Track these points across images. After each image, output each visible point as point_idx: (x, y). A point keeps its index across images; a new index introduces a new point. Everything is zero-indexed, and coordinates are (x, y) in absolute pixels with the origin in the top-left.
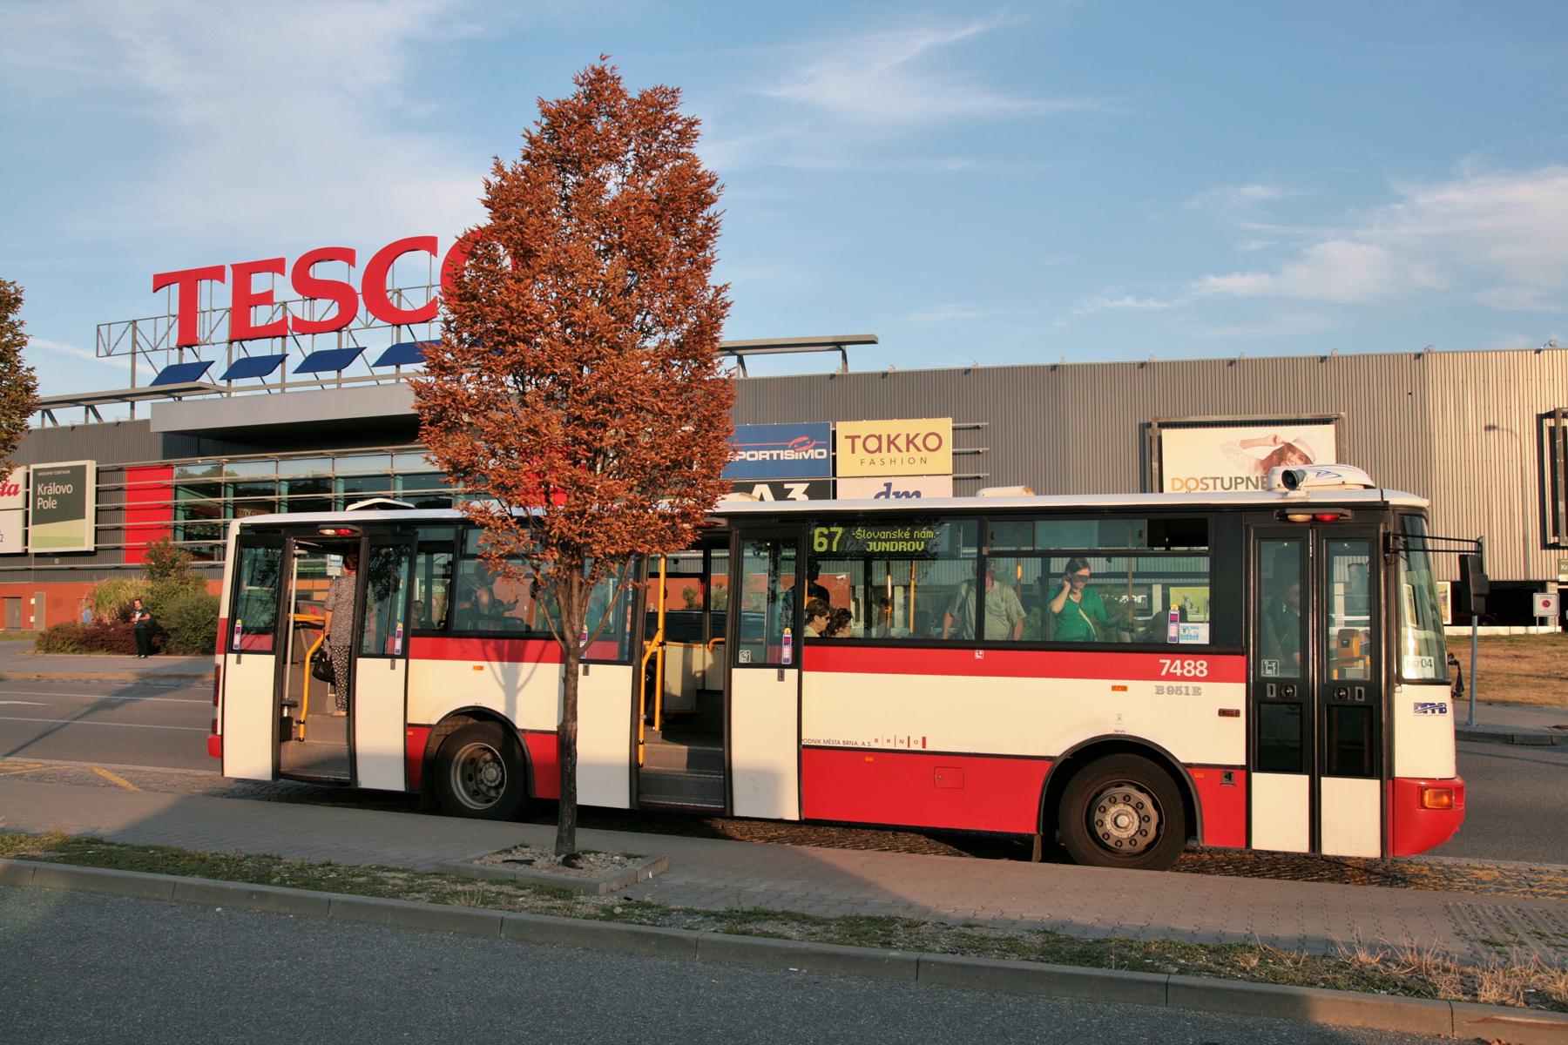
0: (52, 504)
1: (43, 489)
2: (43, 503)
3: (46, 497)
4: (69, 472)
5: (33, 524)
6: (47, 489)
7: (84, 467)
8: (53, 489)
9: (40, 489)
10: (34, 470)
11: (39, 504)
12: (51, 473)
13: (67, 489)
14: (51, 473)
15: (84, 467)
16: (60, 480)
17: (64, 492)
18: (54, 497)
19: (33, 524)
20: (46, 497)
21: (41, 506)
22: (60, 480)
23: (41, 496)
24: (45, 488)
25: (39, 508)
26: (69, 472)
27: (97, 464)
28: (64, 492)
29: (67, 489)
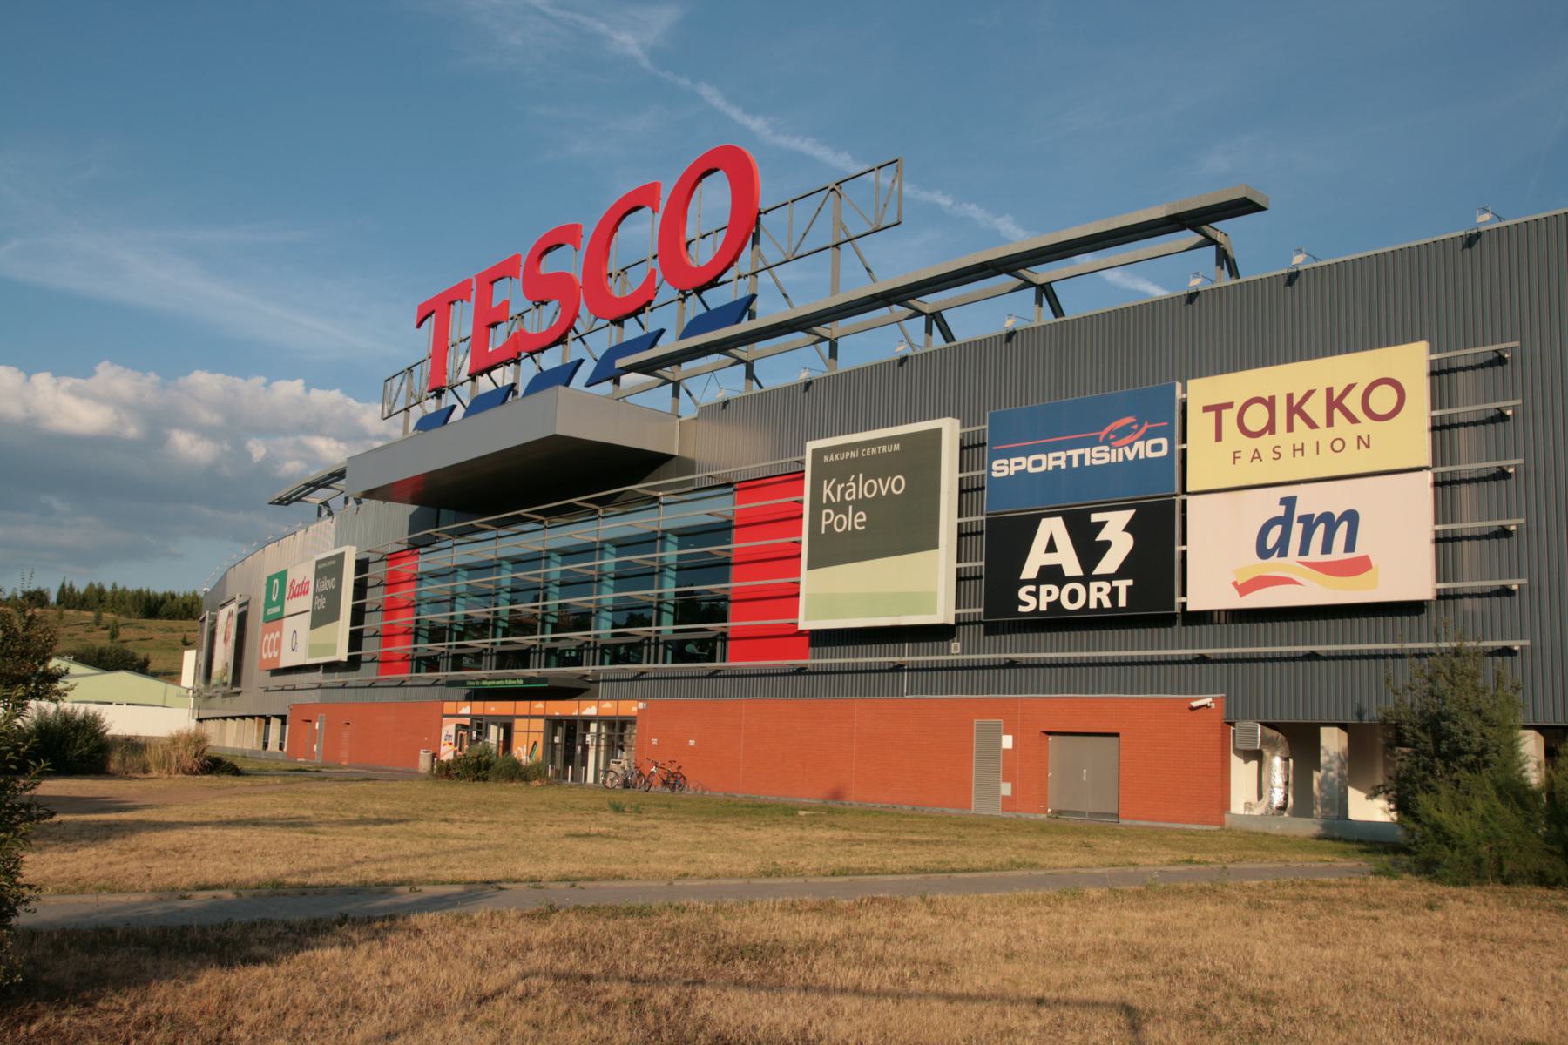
0: (855, 521)
1: (834, 490)
2: (834, 519)
3: (841, 507)
4: (897, 447)
5: (810, 567)
6: (844, 491)
7: (937, 433)
8: (858, 489)
9: (827, 491)
10: (815, 452)
11: (824, 523)
12: (853, 454)
13: (894, 485)
14: (853, 454)
15: (937, 433)
16: (876, 466)
17: (884, 493)
18: (859, 504)
19: (810, 567)
20: (841, 507)
21: (829, 527)
22: (876, 466)
23: (829, 505)
24: (839, 487)
25: (823, 532)
26: (897, 447)
27: (963, 426)
28: (884, 493)
29: (894, 485)
